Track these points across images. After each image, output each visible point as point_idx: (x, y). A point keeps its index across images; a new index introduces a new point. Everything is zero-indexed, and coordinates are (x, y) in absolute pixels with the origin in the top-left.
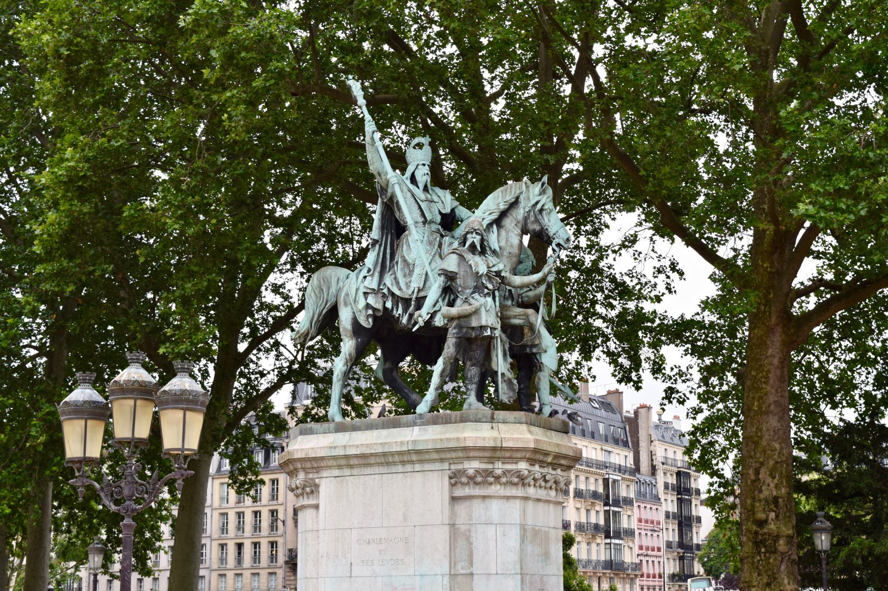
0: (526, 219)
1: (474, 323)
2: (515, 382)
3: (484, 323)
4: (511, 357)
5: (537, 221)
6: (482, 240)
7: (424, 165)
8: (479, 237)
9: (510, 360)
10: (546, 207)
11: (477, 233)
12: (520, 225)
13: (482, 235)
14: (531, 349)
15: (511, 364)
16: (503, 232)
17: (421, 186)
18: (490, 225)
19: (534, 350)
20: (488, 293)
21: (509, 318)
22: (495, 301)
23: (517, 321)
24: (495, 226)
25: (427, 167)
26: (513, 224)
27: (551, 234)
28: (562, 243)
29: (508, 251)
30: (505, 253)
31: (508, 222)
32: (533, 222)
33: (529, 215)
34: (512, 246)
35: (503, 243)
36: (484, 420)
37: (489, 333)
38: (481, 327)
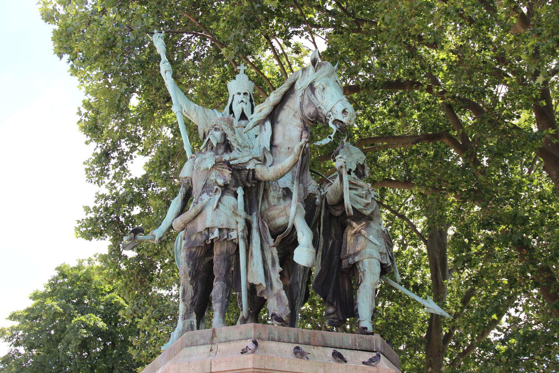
0: (301, 104)
1: (200, 228)
2: (283, 293)
3: (208, 224)
4: (281, 266)
5: (311, 103)
6: (225, 135)
7: (239, 94)
8: (218, 134)
9: (279, 268)
10: (316, 85)
11: (216, 129)
12: (299, 115)
13: (222, 130)
14: (353, 258)
15: (280, 273)
16: (279, 128)
17: (237, 114)
18: (261, 123)
19: (357, 259)
20: (217, 189)
21: (274, 218)
22: (237, 198)
23: (280, 221)
24: (268, 124)
25: (242, 94)
26: (291, 116)
27: (325, 112)
28: (340, 117)
29: (286, 146)
30: (282, 150)
31: (285, 115)
32: (307, 106)
33: (303, 100)
34: (291, 140)
35: (278, 140)
36: (202, 341)
37: (216, 234)
38: (208, 229)
